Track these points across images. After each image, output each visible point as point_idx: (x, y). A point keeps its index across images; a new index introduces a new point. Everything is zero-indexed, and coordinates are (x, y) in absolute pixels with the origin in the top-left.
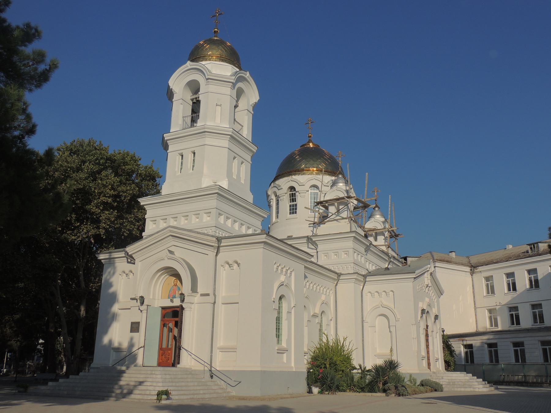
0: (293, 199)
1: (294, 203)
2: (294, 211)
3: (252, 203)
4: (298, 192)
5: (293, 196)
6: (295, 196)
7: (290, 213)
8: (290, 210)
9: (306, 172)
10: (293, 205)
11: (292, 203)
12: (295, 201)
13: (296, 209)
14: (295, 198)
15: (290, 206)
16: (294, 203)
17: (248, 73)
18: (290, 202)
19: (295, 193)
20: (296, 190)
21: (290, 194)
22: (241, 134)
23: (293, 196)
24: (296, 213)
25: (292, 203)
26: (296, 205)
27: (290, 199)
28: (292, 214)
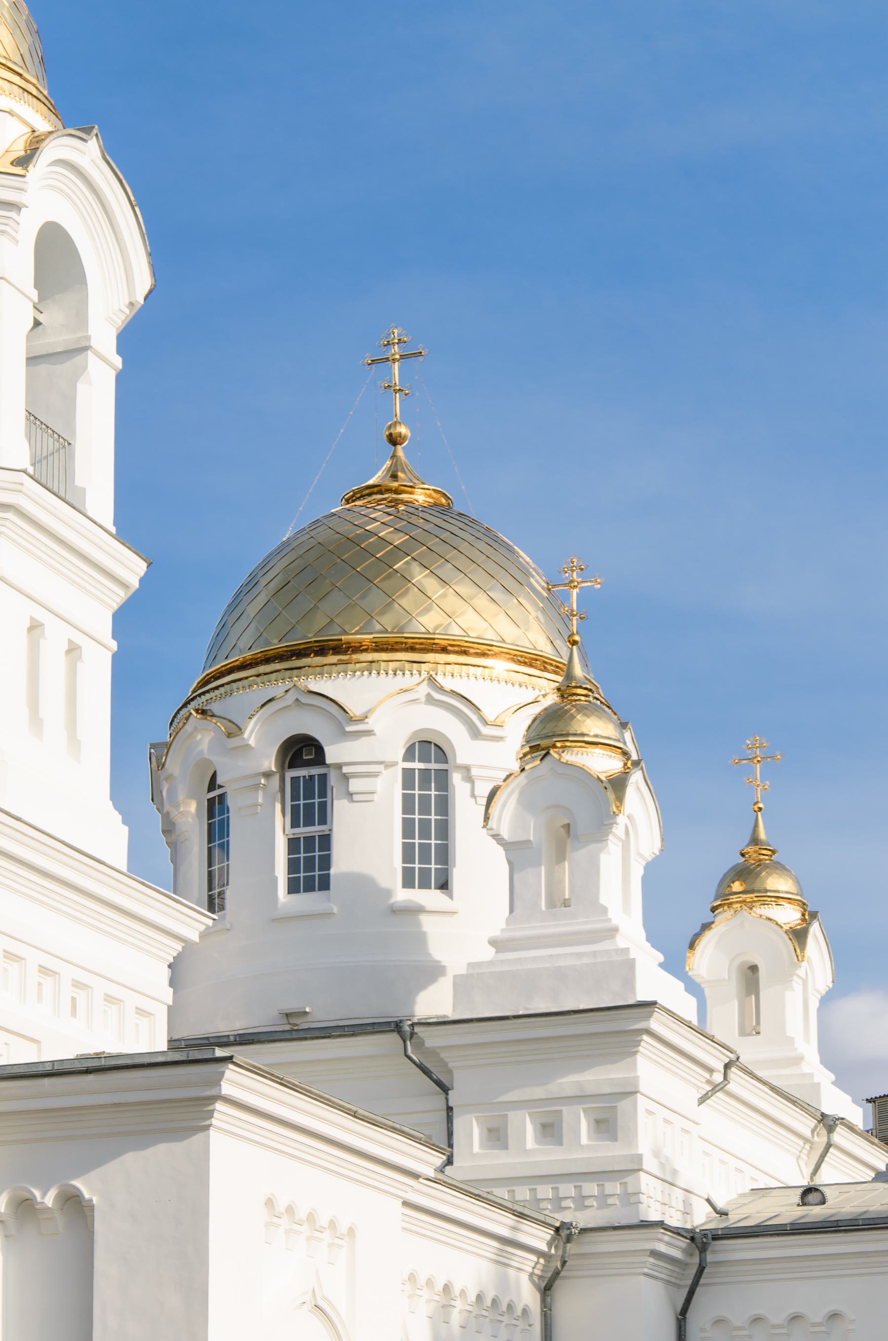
0: (309, 808)
1: (316, 830)
2: (317, 873)
3: (125, 870)
4: (339, 766)
5: (309, 795)
6: (323, 793)
7: (293, 887)
8: (293, 865)
9: (384, 656)
10: (309, 840)
11: (303, 831)
12: (323, 820)
13: (326, 862)
14: (323, 807)
15: (293, 845)
16: (316, 830)
17: (93, 147)
18: (295, 824)
19: (323, 778)
20: (328, 761)
21: (295, 780)
22: (62, 494)
23: (309, 795)
24: (325, 884)
25: (303, 831)
26: (326, 841)
27: (295, 810)
28: (305, 891)
